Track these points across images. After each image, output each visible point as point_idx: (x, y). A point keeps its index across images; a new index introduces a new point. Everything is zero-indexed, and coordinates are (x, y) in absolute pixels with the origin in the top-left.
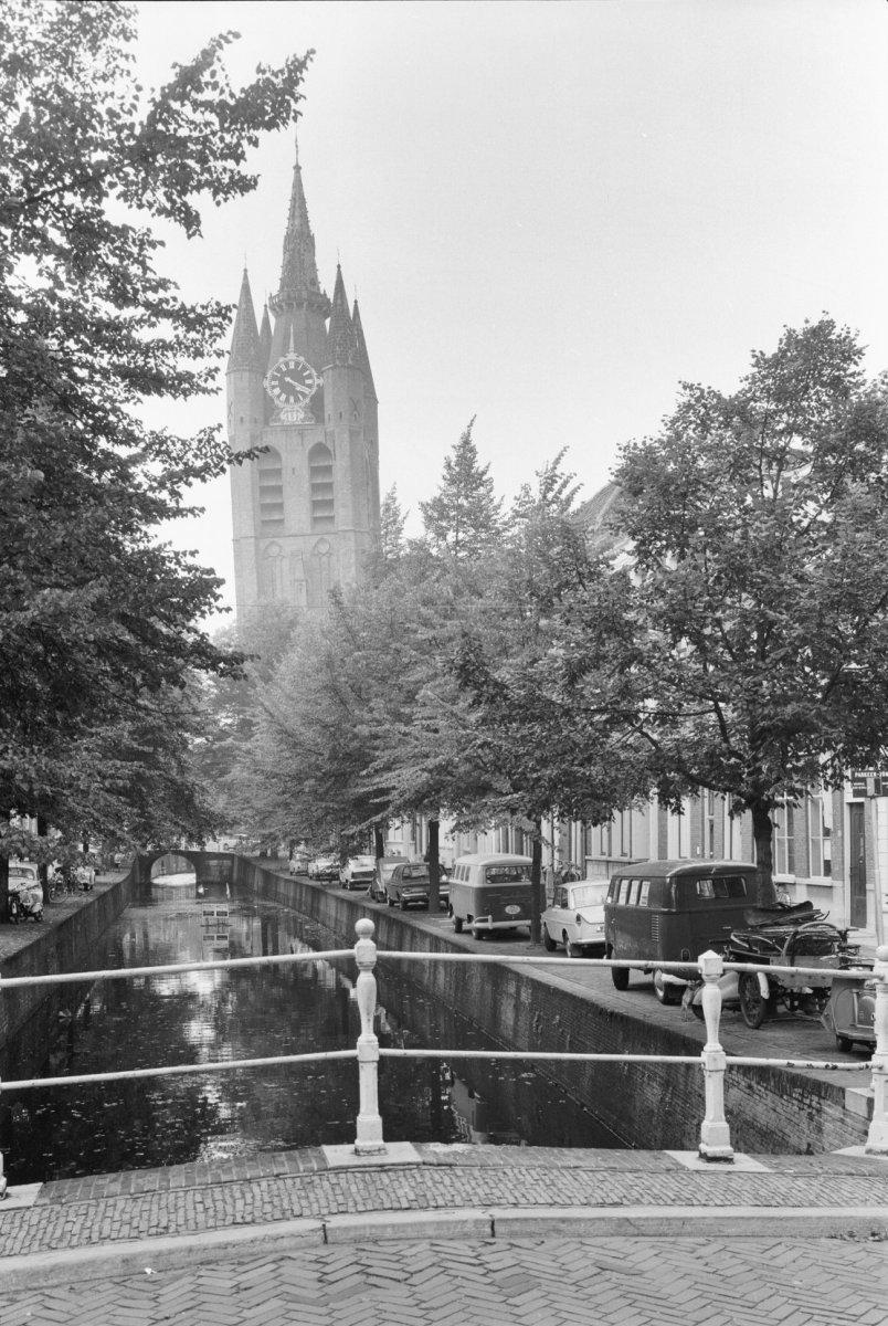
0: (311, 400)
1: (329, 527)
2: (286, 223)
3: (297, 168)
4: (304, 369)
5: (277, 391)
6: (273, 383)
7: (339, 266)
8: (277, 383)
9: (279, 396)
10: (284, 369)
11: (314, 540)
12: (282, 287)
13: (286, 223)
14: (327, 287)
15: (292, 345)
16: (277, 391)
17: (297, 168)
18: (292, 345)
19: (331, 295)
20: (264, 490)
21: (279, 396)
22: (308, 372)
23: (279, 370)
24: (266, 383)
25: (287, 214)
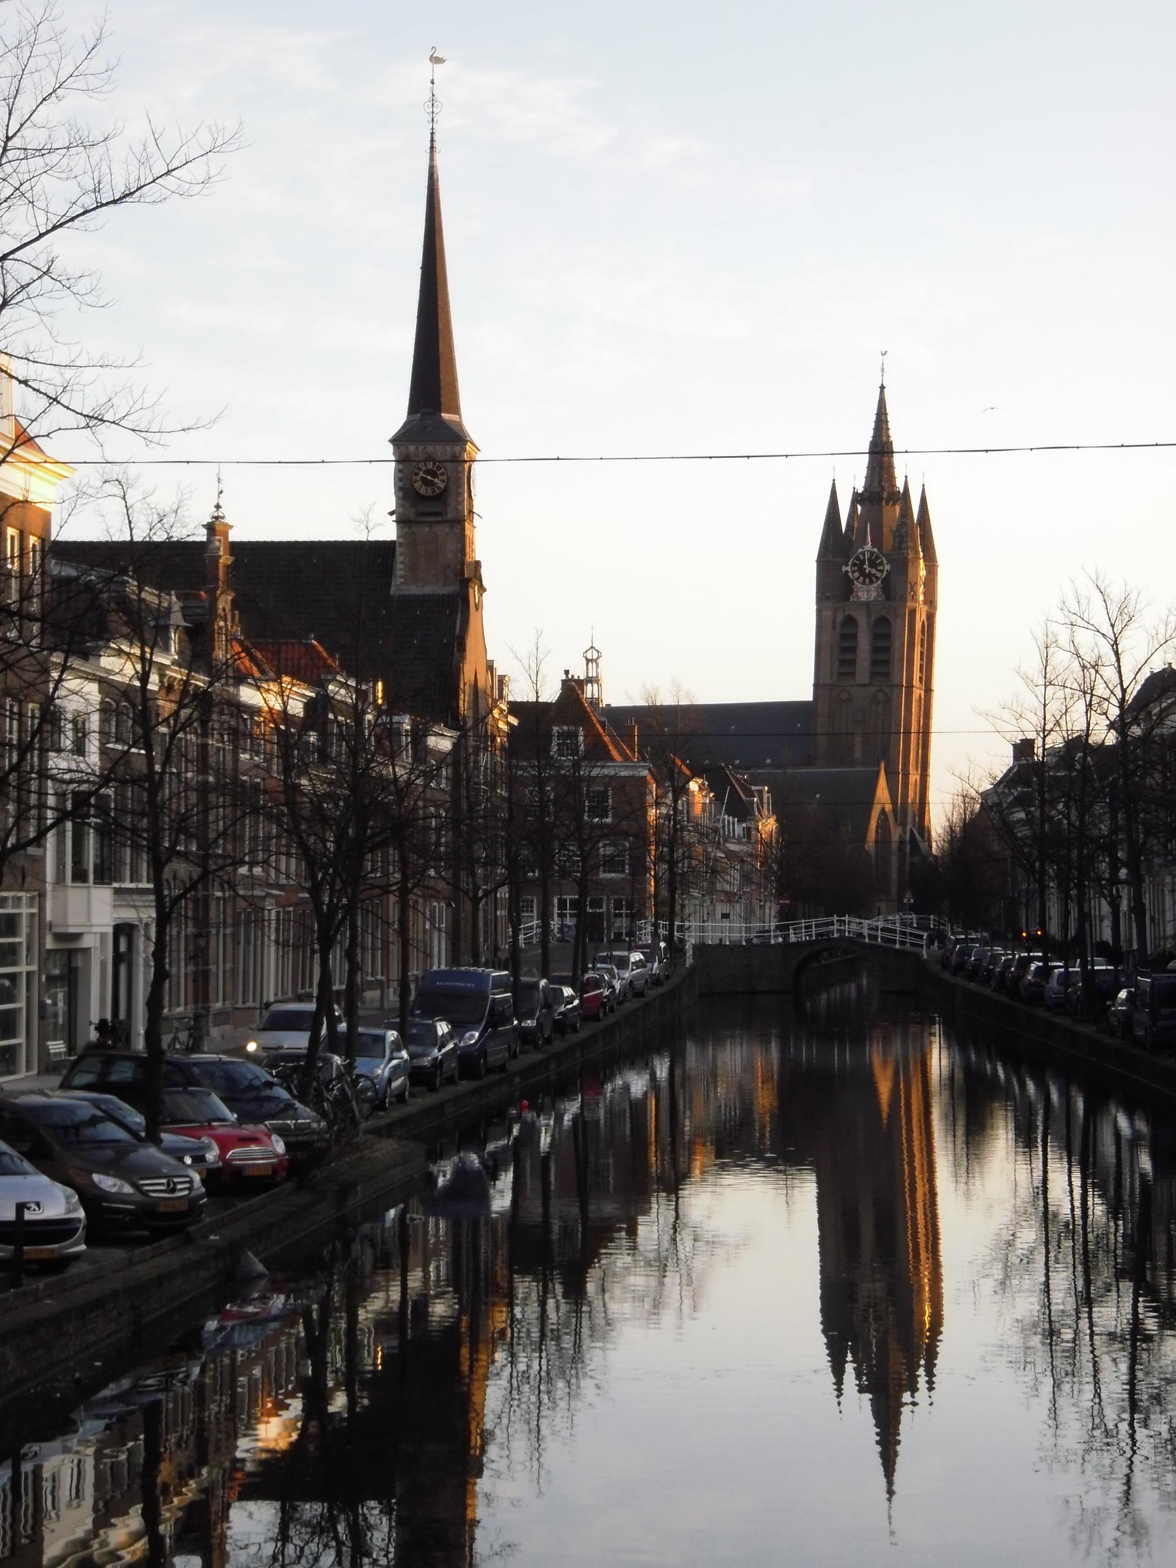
3: (882, 388)
4: (877, 557)
5: (857, 574)
8: (856, 568)
9: (858, 578)
13: (871, 433)
14: (900, 485)
16: (857, 574)
17: (882, 388)
19: (901, 491)
20: (844, 650)
21: (858, 578)
23: (858, 558)
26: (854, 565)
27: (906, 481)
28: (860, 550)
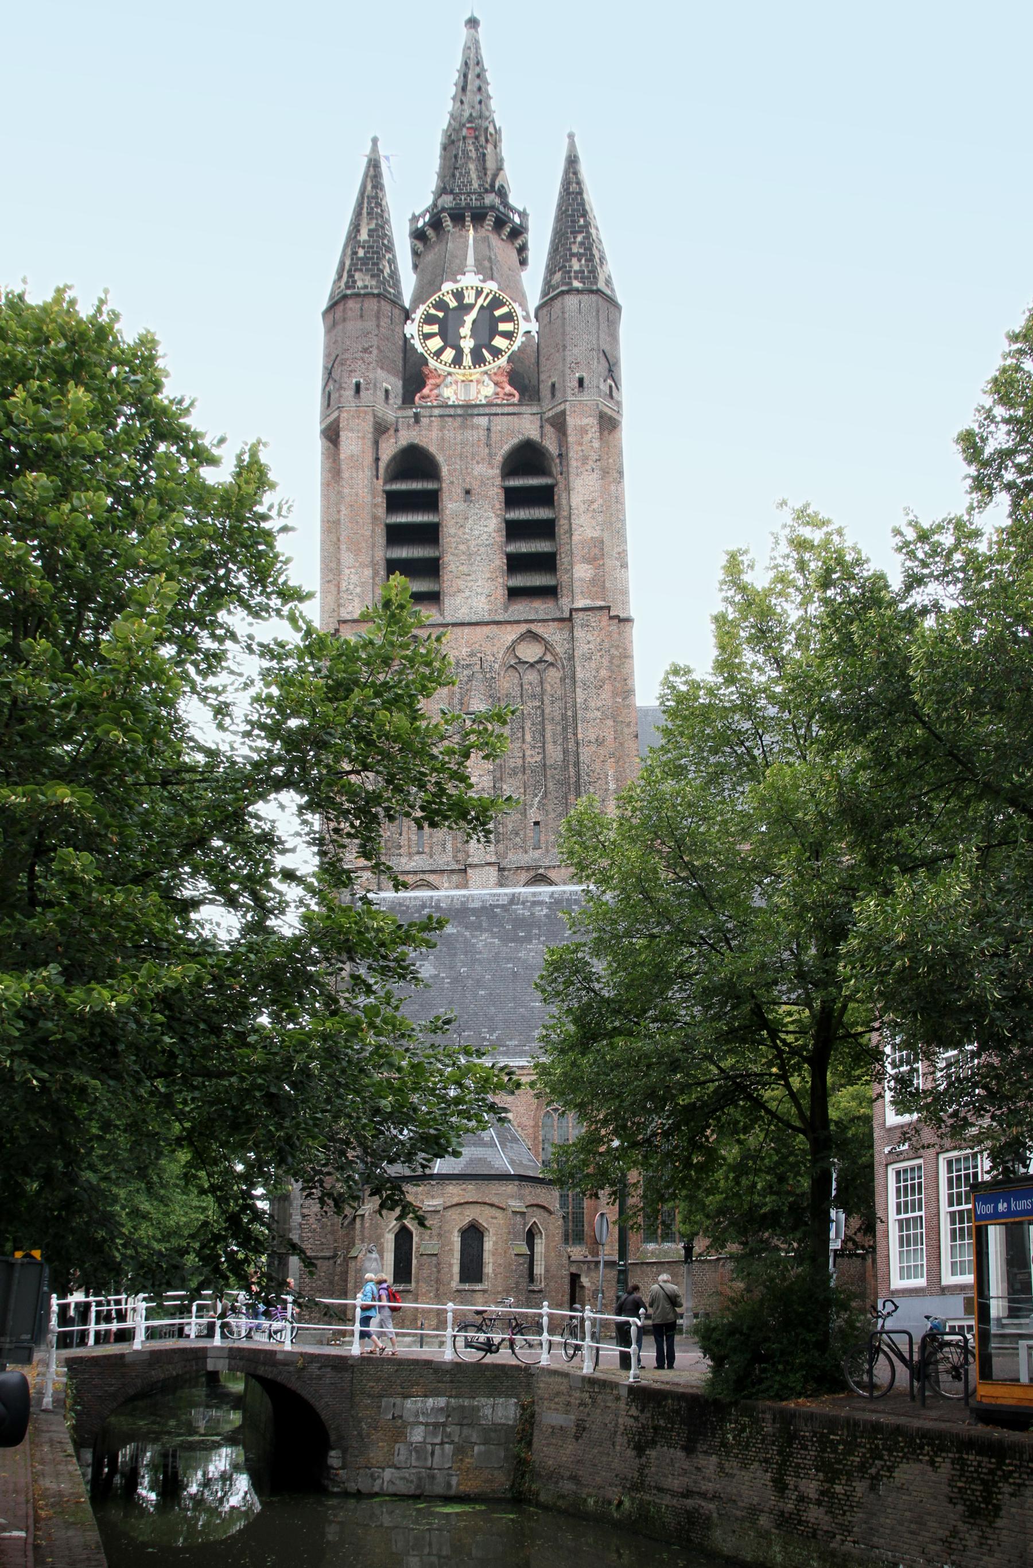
0: (509, 360)
1: (540, 608)
2: (450, 106)
3: (473, 23)
5: (436, 343)
6: (427, 329)
7: (571, 136)
8: (435, 328)
9: (438, 353)
10: (453, 304)
11: (510, 634)
12: (442, 191)
15: (471, 260)
16: (436, 343)
17: (473, 23)
18: (471, 260)
21: (438, 353)
22: (504, 310)
23: (441, 305)
24: (411, 329)
25: (453, 90)
26: (429, 319)
27: (572, 145)
28: (447, 286)
